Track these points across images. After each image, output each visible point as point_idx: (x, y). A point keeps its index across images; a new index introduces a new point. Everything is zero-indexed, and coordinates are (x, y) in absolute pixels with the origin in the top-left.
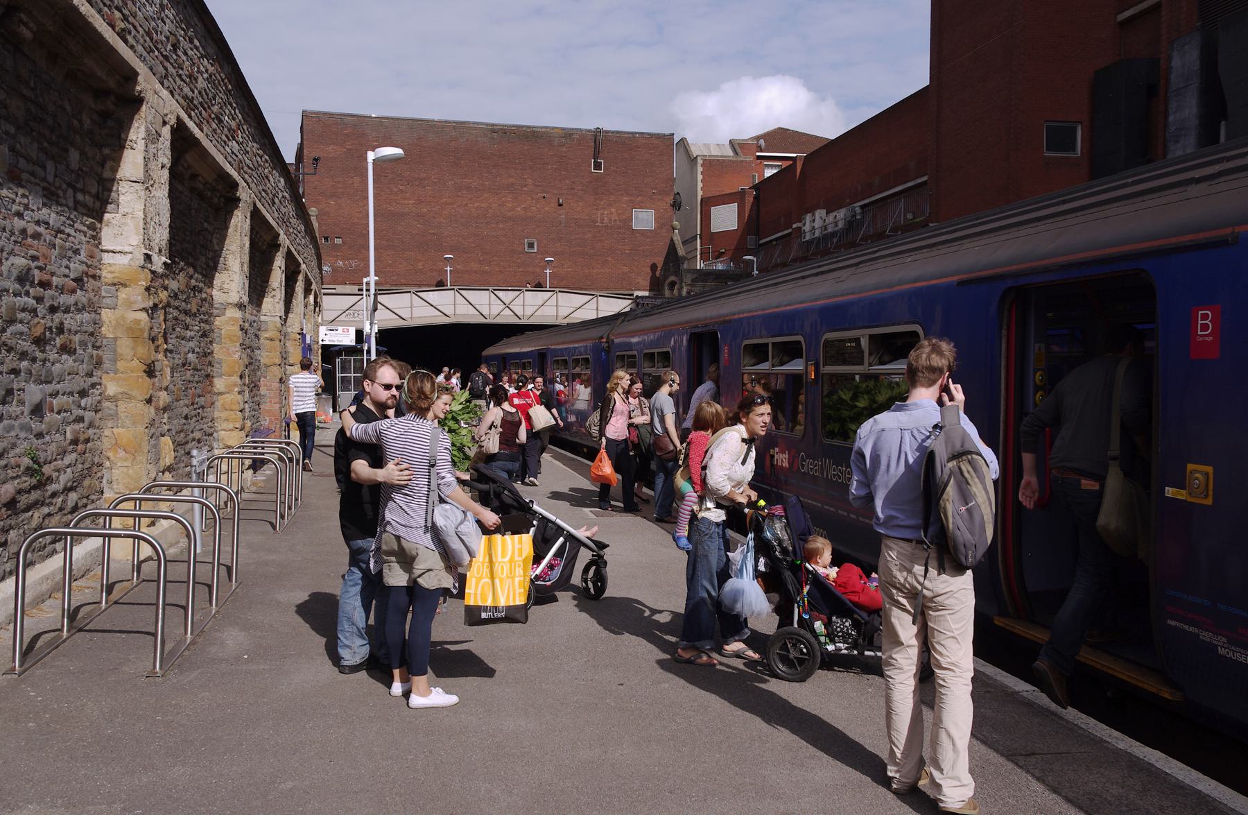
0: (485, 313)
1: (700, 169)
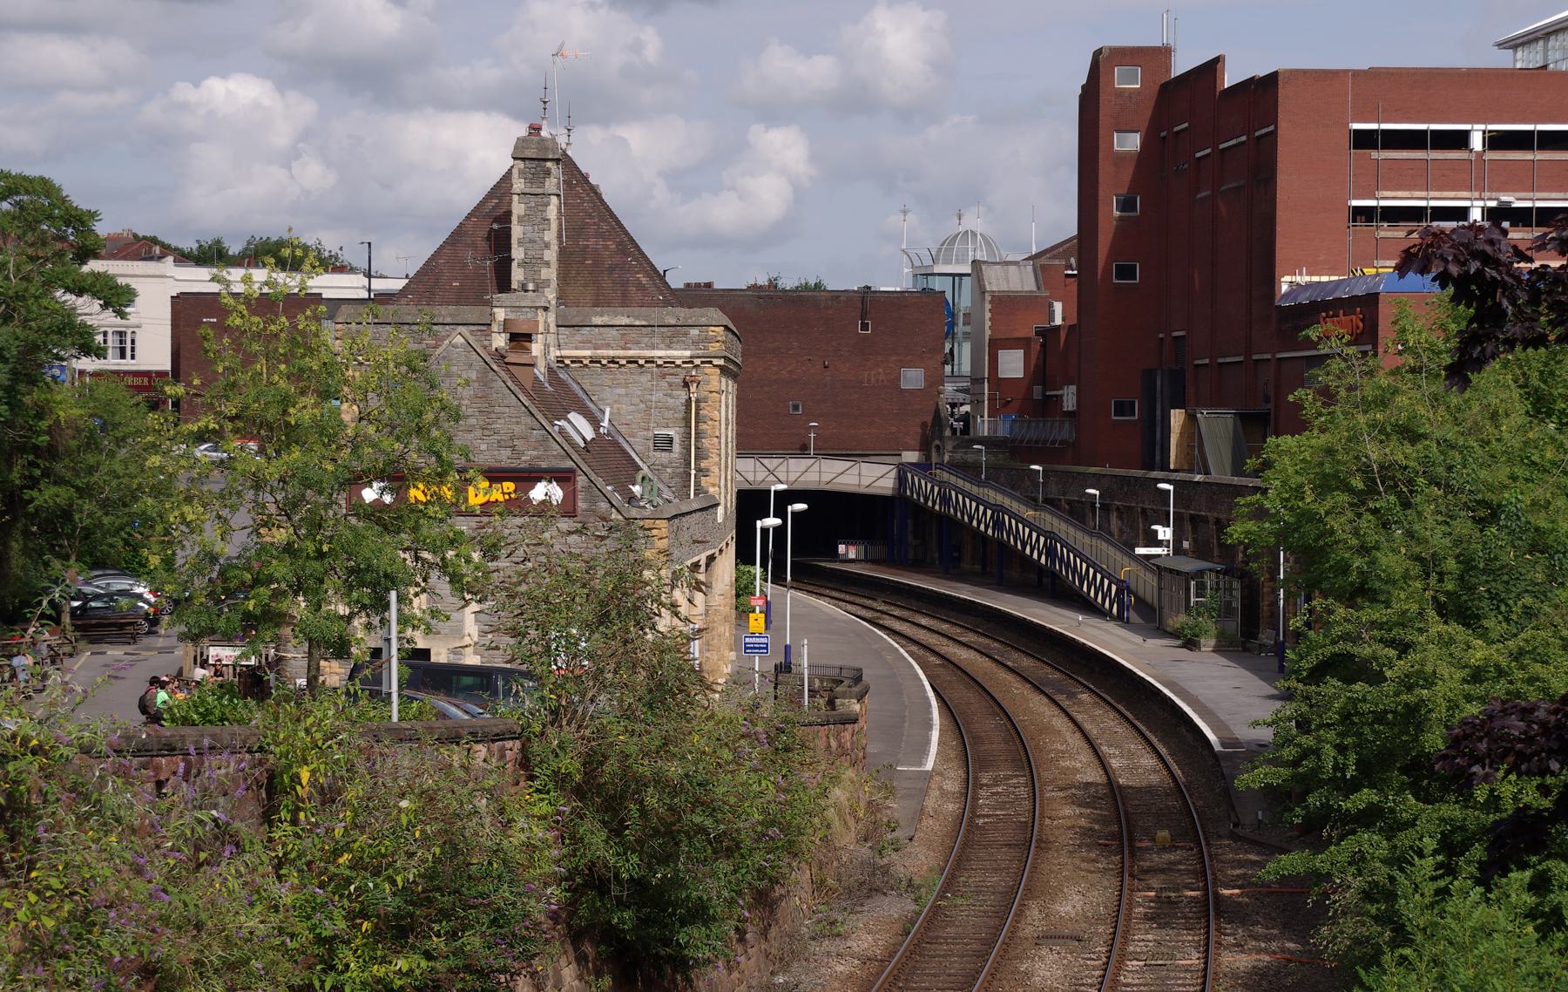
0: (751, 478)
1: (988, 306)
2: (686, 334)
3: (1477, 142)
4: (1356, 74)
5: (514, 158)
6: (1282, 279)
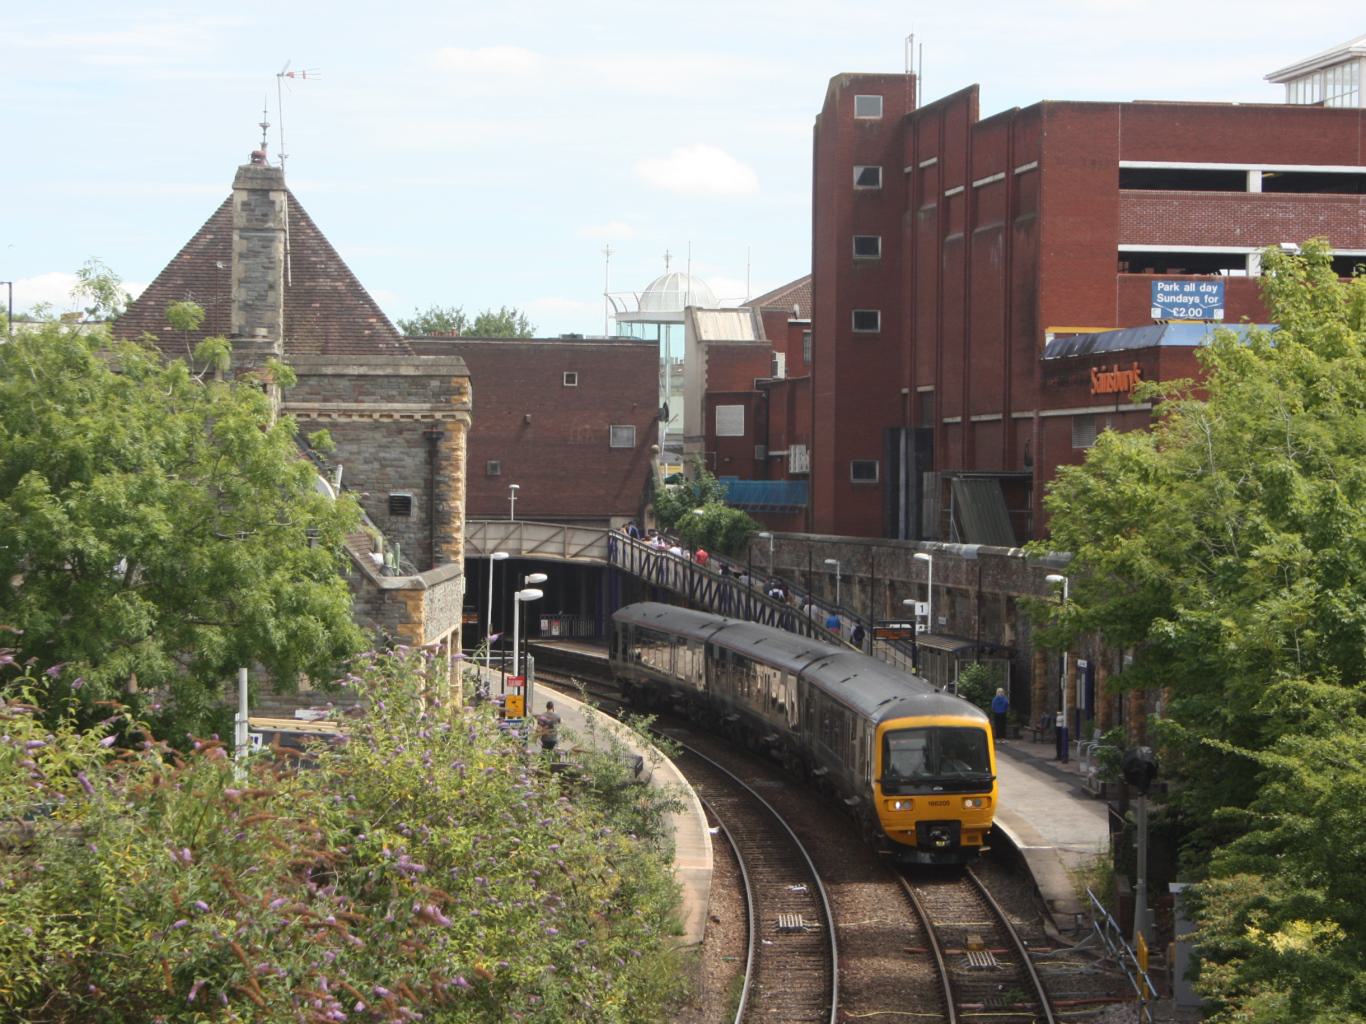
2: (424, 387)
3: (1255, 184)
4: (1126, 107)
5: (234, 189)
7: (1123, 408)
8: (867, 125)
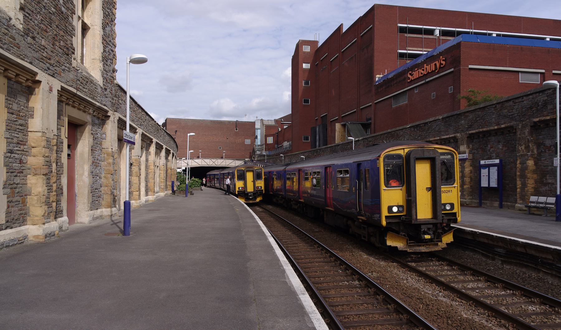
3: (437, 33)
4: (400, 7)
6: (376, 76)
7: (427, 80)
8: (306, 53)
